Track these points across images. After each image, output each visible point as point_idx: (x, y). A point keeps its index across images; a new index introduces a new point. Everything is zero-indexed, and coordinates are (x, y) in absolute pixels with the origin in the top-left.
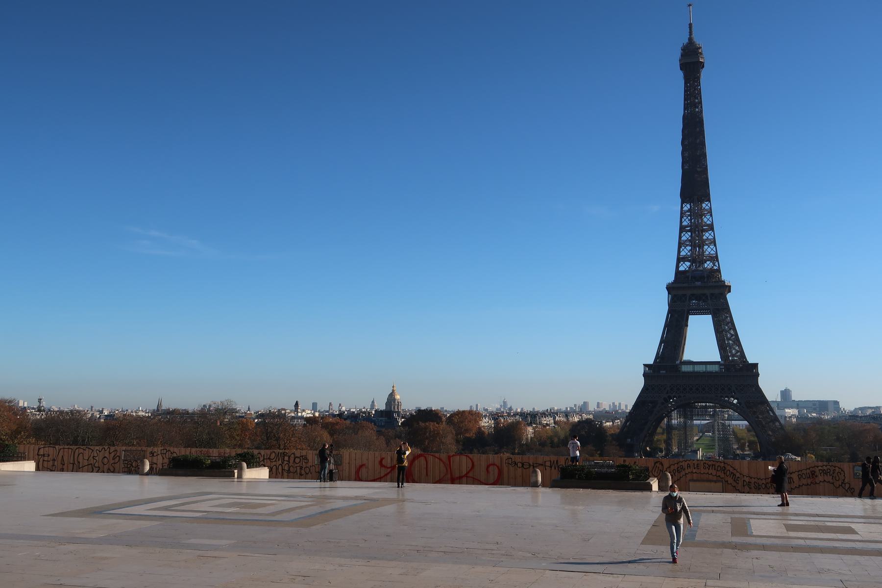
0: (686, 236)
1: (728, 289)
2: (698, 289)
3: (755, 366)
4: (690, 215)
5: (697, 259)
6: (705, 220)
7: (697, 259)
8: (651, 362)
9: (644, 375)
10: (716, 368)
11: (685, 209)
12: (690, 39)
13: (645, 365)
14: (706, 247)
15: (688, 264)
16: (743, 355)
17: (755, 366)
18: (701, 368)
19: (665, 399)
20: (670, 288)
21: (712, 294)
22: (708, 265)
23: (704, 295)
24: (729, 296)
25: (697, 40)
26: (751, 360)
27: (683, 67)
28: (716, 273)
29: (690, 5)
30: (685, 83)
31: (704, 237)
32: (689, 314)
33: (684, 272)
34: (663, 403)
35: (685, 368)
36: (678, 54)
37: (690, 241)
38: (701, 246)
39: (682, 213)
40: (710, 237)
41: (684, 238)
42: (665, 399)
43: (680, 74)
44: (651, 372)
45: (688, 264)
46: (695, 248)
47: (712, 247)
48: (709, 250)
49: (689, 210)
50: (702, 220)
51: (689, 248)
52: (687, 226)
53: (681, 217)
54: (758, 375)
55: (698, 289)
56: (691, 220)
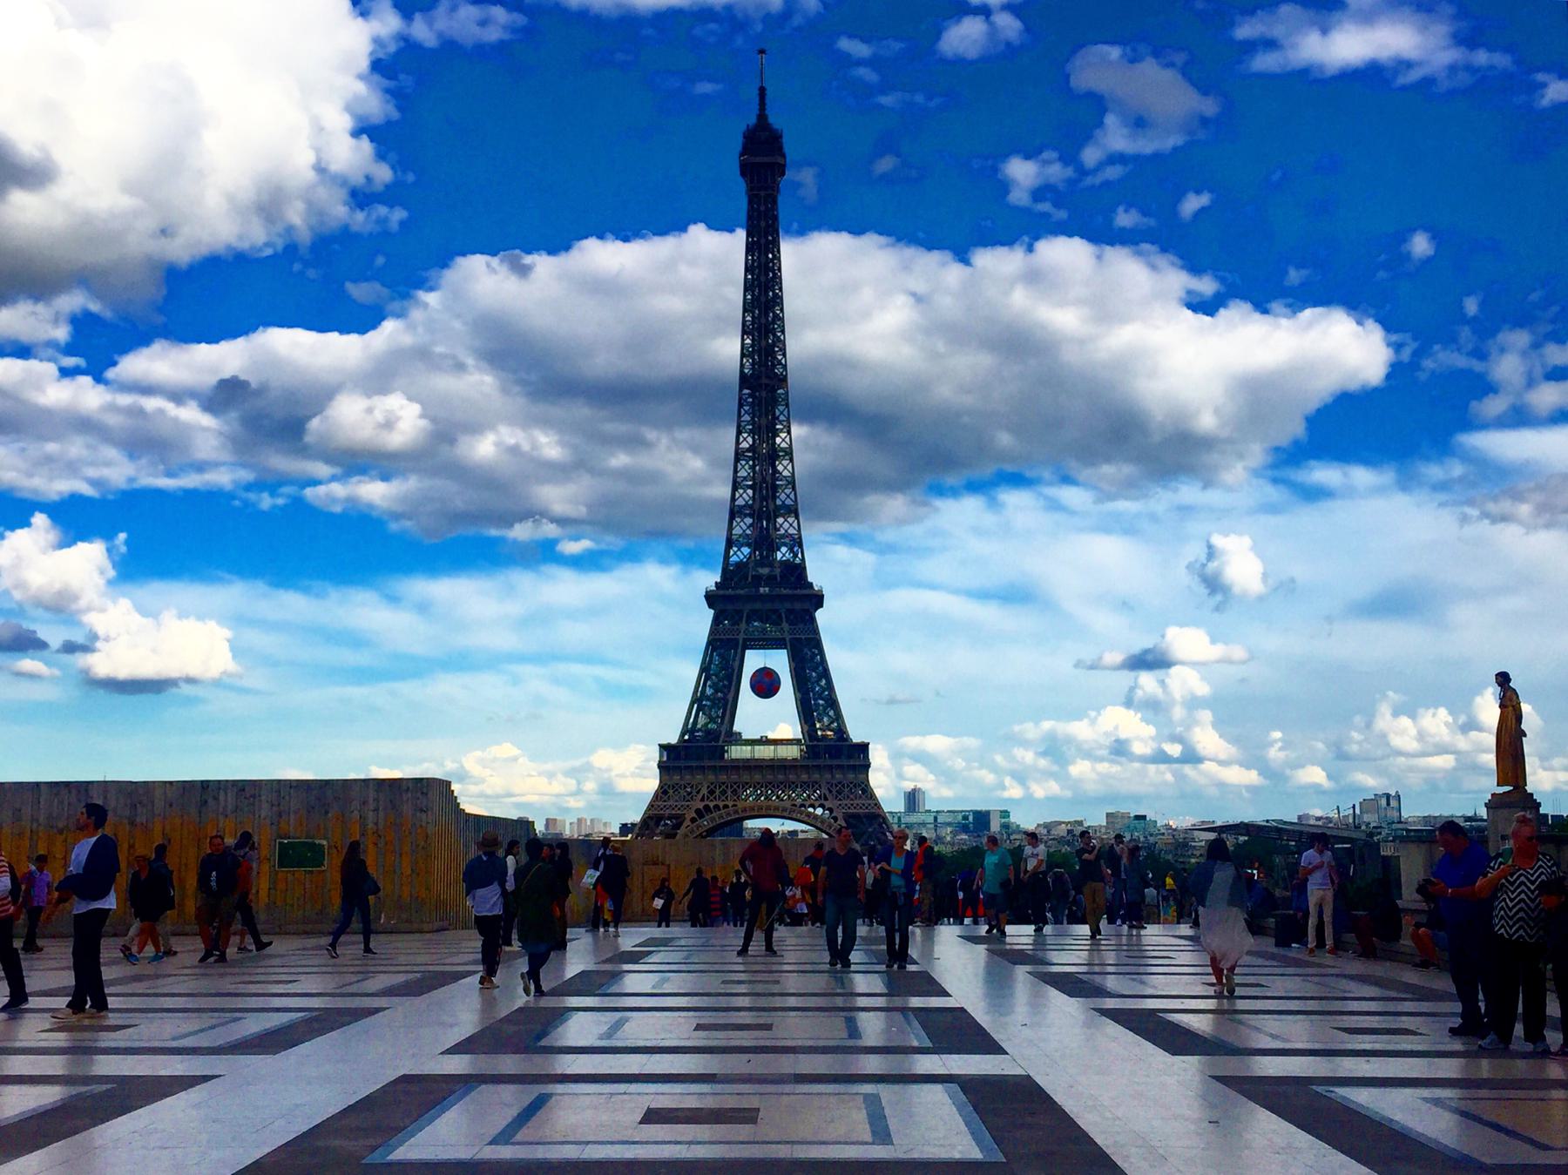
0: (745, 496)
1: (818, 600)
2: (764, 603)
3: (863, 748)
4: (753, 459)
5: (764, 542)
6: (780, 468)
7: (764, 542)
8: (674, 740)
9: (660, 766)
10: (792, 752)
11: (745, 445)
12: (762, 116)
13: (664, 748)
14: (780, 520)
15: (746, 550)
16: (841, 732)
17: (863, 748)
18: (765, 752)
19: (698, 811)
20: (710, 598)
21: (790, 611)
22: (782, 554)
23: (775, 611)
24: (820, 615)
25: (775, 120)
26: (856, 737)
27: (746, 170)
28: (797, 572)
29: (762, 52)
30: (750, 202)
31: (778, 502)
32: (746, 647)
33: (739, 565)
34: (693, 820)
35: (737, 752)
36: (737, 143)
37: (751, 507)
38: (771, 517)
39: (737, 453)
40: (789, 502)
41: (740, 502)
42: (698, 811)
43: (740, 186)
44: (674, 759)
45: (746, 550)
46: (760, 519)
47: (791, 520)
48: (786, 525)
49: (750, 449)
50: (774, 467)
51: (749, 521)
52: (745, 479)
53: (737, 460)
54: (866, 766)
55: (764, 603)
56: (752, 468)
